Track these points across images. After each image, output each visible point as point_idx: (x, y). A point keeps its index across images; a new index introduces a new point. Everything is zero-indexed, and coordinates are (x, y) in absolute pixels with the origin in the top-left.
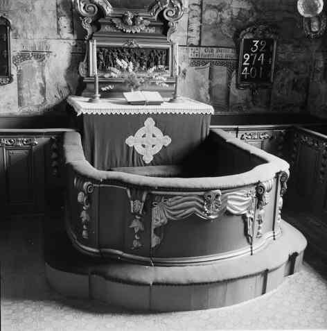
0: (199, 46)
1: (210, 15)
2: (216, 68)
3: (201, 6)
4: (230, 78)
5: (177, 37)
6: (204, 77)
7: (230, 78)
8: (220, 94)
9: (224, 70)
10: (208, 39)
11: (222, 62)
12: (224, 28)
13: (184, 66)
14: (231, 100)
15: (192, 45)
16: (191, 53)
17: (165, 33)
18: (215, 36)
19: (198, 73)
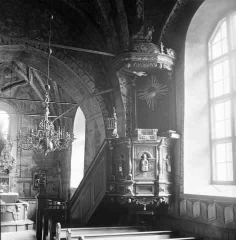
0: (20, 177)
1: (23, 168)
2: (26, 184)
3: (20, 166)
4: (30, 187)
5: (12, 174)
6: (22, 187)
7: (30, 187)
8: (27, 192)
9: (28, 184)
10: (23, 175)
11: (28, 182)
12: (29, 172)
13: (15, 183)
14: (31, 193)
15: (17, 177)
16: (17, 179)
17: (8, 173)
18: (25, 174)
19: (20, 185)
